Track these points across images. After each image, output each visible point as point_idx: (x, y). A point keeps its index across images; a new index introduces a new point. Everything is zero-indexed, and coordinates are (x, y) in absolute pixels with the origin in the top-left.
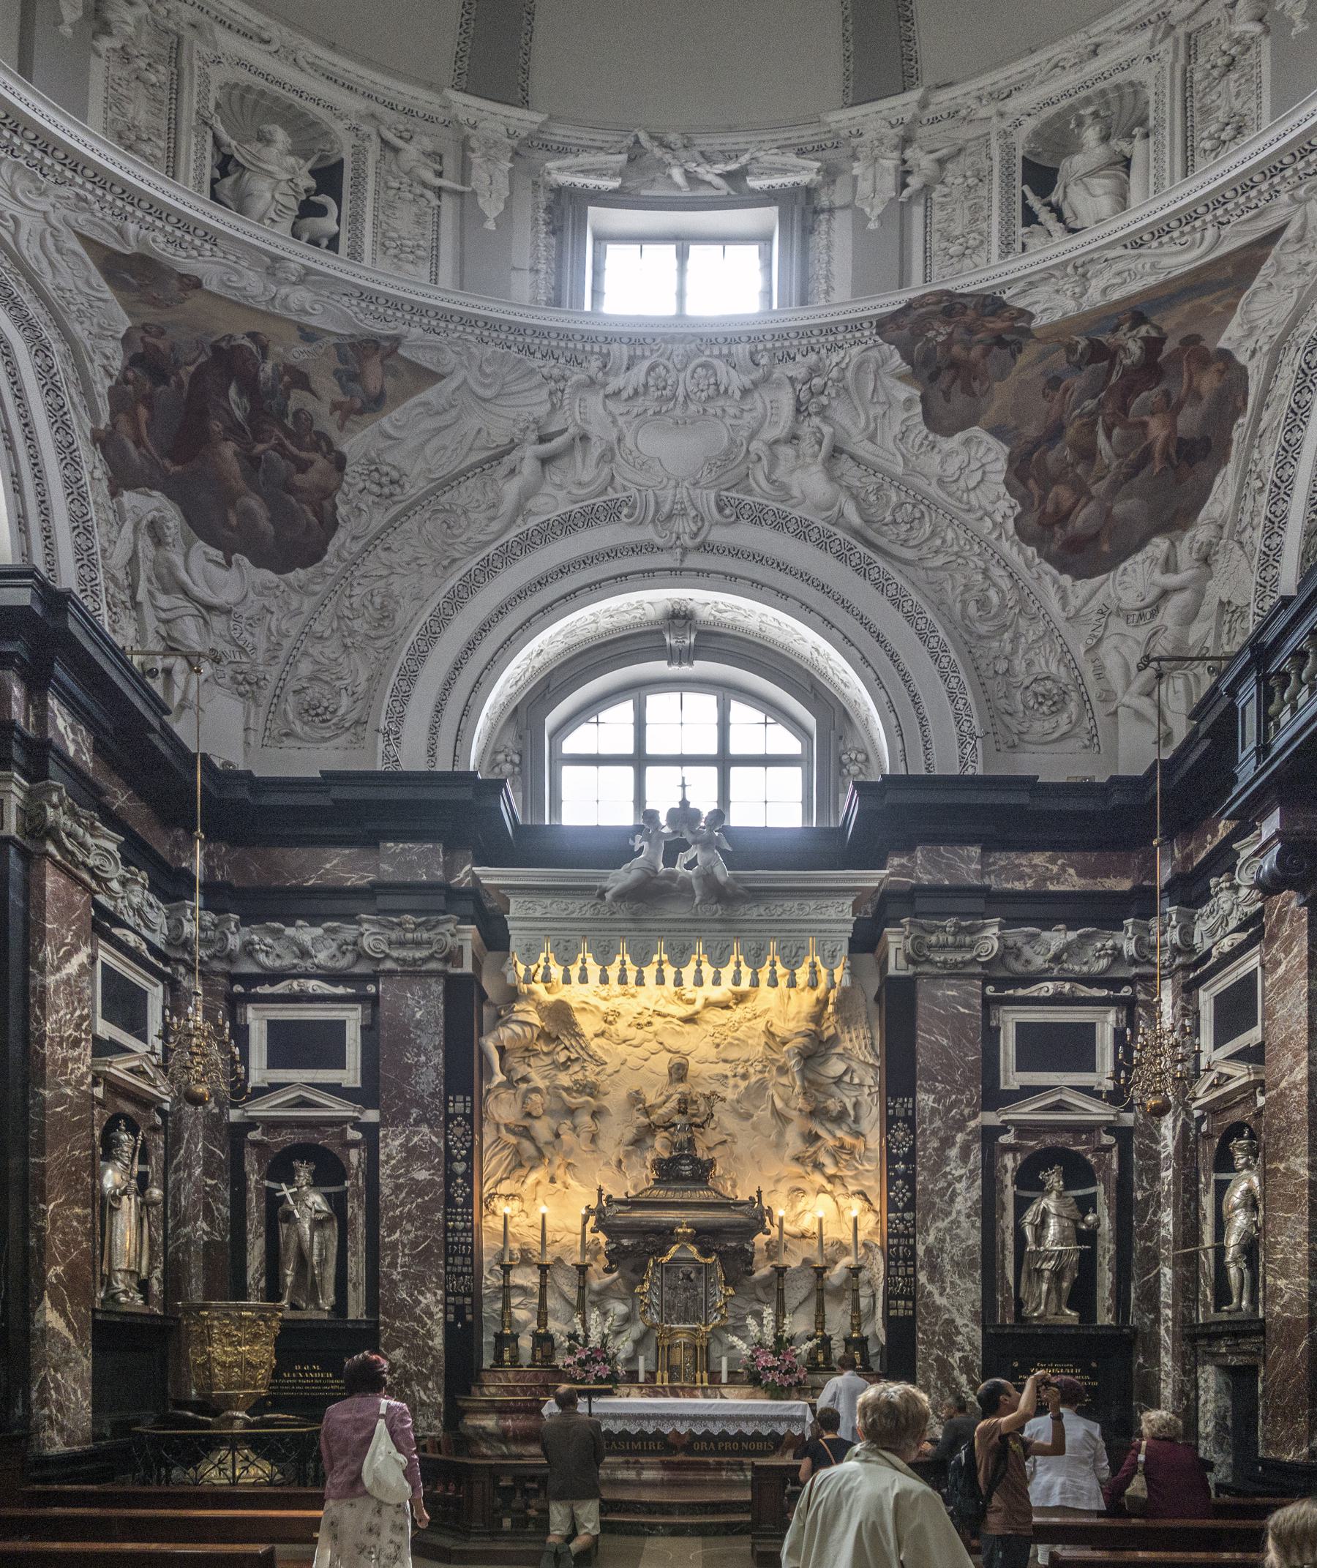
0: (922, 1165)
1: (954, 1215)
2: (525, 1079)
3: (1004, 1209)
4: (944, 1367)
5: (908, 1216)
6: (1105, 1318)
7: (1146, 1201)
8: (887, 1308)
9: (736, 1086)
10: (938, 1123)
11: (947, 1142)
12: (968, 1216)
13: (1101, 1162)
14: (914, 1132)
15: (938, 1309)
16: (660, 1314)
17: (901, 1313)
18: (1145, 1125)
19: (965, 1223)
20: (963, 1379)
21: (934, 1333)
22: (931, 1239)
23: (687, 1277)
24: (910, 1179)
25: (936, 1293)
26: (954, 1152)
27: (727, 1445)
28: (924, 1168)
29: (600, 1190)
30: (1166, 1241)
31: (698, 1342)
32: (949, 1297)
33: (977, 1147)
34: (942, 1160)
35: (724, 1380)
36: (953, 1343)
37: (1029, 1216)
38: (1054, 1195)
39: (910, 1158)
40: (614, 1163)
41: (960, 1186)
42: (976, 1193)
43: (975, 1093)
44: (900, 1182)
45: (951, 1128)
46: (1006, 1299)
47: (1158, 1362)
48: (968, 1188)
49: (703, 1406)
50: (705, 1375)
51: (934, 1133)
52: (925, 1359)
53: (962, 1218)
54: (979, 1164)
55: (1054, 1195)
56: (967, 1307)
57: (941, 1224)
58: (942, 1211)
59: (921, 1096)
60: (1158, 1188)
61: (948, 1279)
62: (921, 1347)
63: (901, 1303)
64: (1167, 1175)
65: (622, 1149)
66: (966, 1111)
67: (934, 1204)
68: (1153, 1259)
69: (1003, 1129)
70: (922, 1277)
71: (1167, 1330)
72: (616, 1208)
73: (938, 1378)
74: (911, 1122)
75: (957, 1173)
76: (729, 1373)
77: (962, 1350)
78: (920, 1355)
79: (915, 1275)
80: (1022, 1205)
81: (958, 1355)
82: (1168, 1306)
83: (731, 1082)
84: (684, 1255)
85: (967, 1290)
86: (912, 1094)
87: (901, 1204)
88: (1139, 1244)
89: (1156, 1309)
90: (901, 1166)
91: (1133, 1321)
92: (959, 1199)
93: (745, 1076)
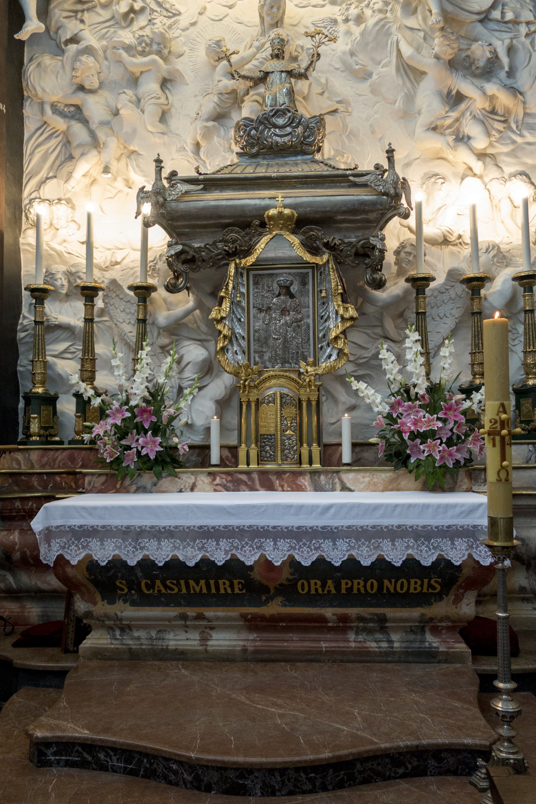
2: (74, 40)
9: (348, 33)
16: (247, 353)
23: (286, 290)
27: (358, 584)
29: (158, 161)
31: (304, 393)
35: (347, 457)
40: (189, 147)
49: (313, 508)
50: (316, 449)
65: (200, 124)
72: (183, 188)
76: (354, 445)
83: (342, 28)
84: (280, 253)
93: (359, 19)
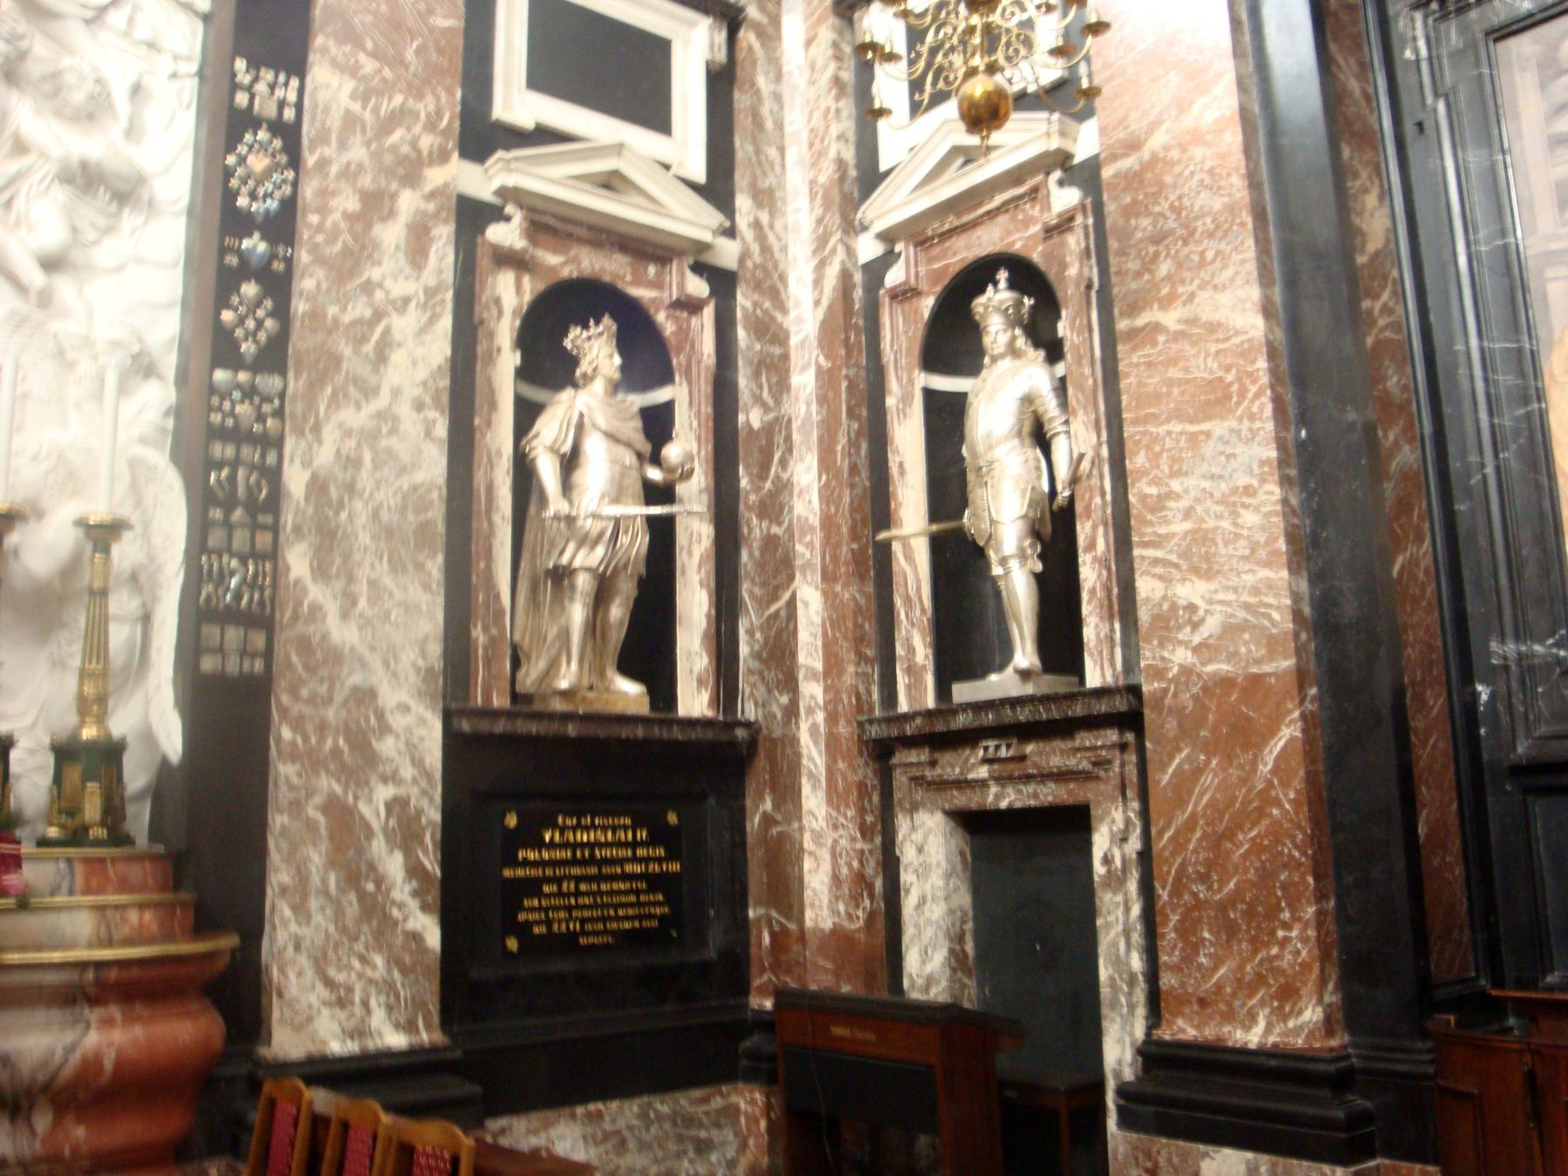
0: (315, 249)
1: (382, 401)
3: (493, 405)
4: (346, 828)
5: (271, 383)
6: (694, 701)
7: (769, 430)
8: (190, 648)
10: (357, 153)
11: (376, 205)
12: (419, 406)
13: (684, 333)
14: (295, 162)
15: (336, 657)
17: (233, 666)
18: (763, 267)
19: (411, 423)
20: (394, 865)
21: (322, 727)
22: (325, 455)
24: (278, 286)
25: (332, 609)
26: (391, 234)
28: (319, 260)
30: (806, 528)
32: (365, 623)
33: (444, 235)
34: (360, 252)
36: (370, 758)
37: (550, 430)
38: (598, 386)
39: (282, 225)
41: (404, 325)
42: (439, 347)
43: (446, 102)
44: (250, 289)
45: (390, 173)
46: (493, 643)
47: (796, 812)
48: (422, 331)
51: (350, 174)
52: (296, 807)
53: (405, 410)
54: (449, 276)
55: (598, 386)
56: (409, 658)
57: (356, 417)
58: (358, 382)
59: (321, 74)
60: (787, 408)
61: (363, 574)
62: (285, 771)
63: (233, 635)
64: (804, 381)
66: (427, 142)
67: (337, 361)
68: (779, 566)
69: (494, 213)
70: (298, 561)
71: (814, 730)
73: (331, 864)
74: (289, 135)
75: (400, 288)
77: (392, 778)
78: (280, 794)
79: (274, 555)
80: (527, 414)
81: (384, 793)
82: (813, 675)
85: (409, 608)
86: (296, 65)
87: (248, 348)
88: (754, 529)
89: (790, 683)
90: (255, 245)
91: (749, 711)
92: (398, 357)
